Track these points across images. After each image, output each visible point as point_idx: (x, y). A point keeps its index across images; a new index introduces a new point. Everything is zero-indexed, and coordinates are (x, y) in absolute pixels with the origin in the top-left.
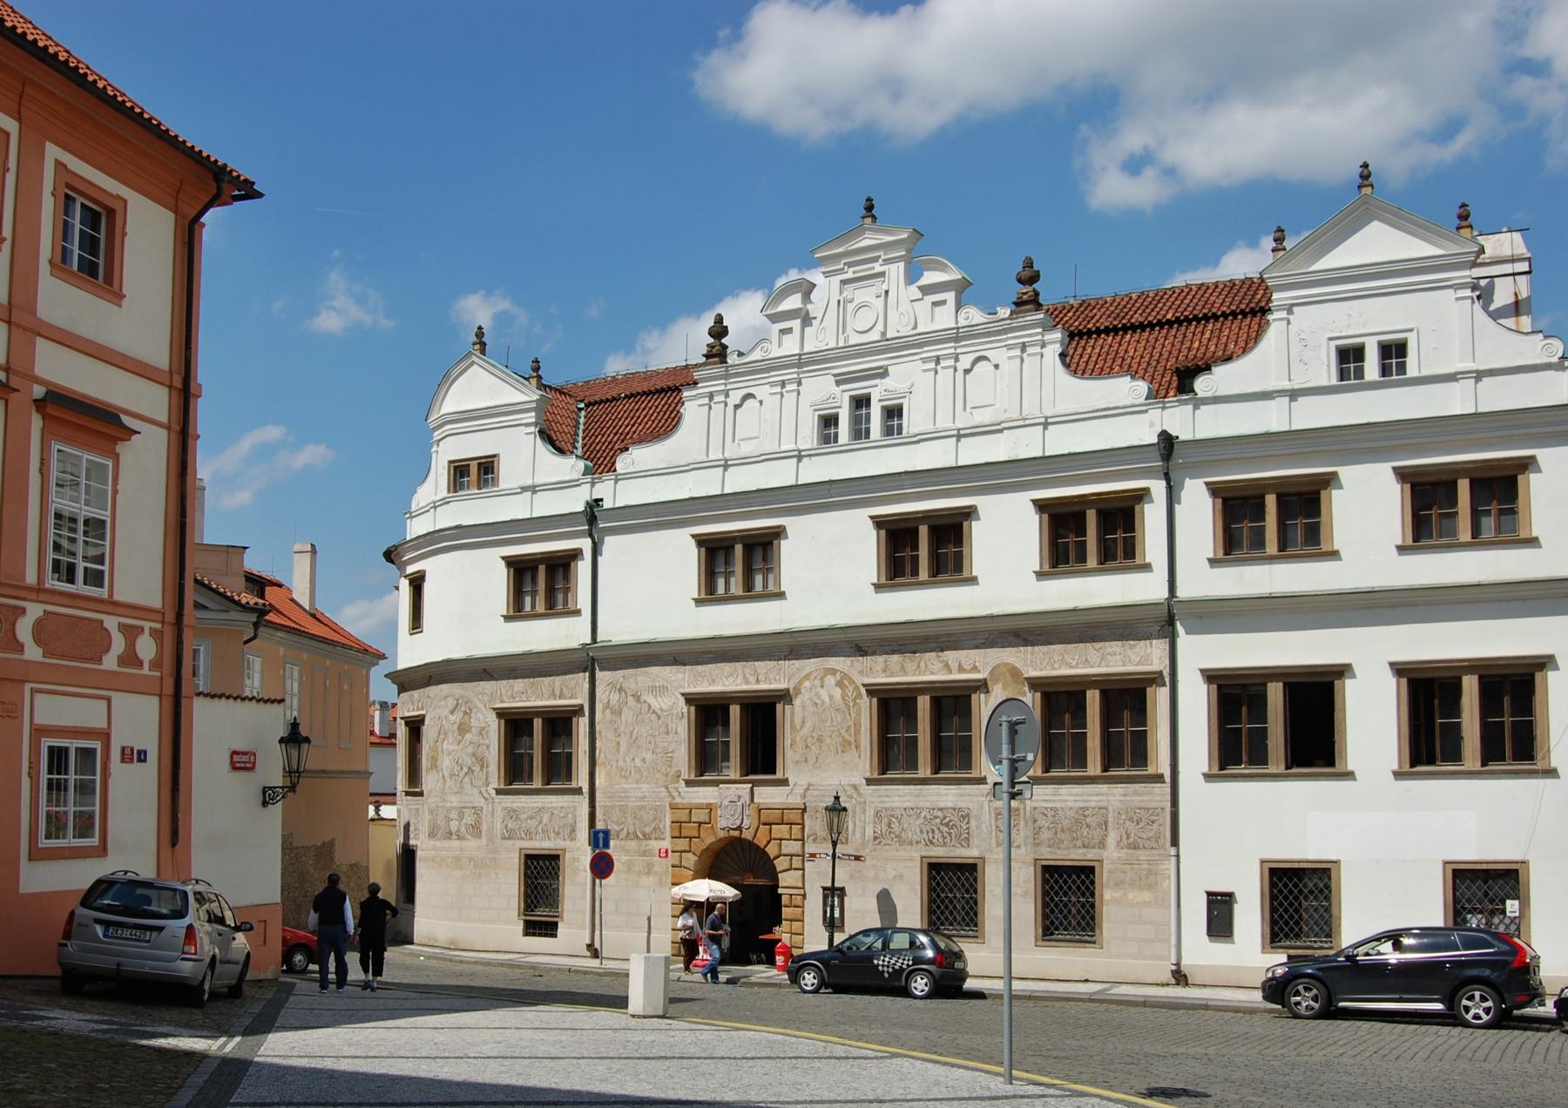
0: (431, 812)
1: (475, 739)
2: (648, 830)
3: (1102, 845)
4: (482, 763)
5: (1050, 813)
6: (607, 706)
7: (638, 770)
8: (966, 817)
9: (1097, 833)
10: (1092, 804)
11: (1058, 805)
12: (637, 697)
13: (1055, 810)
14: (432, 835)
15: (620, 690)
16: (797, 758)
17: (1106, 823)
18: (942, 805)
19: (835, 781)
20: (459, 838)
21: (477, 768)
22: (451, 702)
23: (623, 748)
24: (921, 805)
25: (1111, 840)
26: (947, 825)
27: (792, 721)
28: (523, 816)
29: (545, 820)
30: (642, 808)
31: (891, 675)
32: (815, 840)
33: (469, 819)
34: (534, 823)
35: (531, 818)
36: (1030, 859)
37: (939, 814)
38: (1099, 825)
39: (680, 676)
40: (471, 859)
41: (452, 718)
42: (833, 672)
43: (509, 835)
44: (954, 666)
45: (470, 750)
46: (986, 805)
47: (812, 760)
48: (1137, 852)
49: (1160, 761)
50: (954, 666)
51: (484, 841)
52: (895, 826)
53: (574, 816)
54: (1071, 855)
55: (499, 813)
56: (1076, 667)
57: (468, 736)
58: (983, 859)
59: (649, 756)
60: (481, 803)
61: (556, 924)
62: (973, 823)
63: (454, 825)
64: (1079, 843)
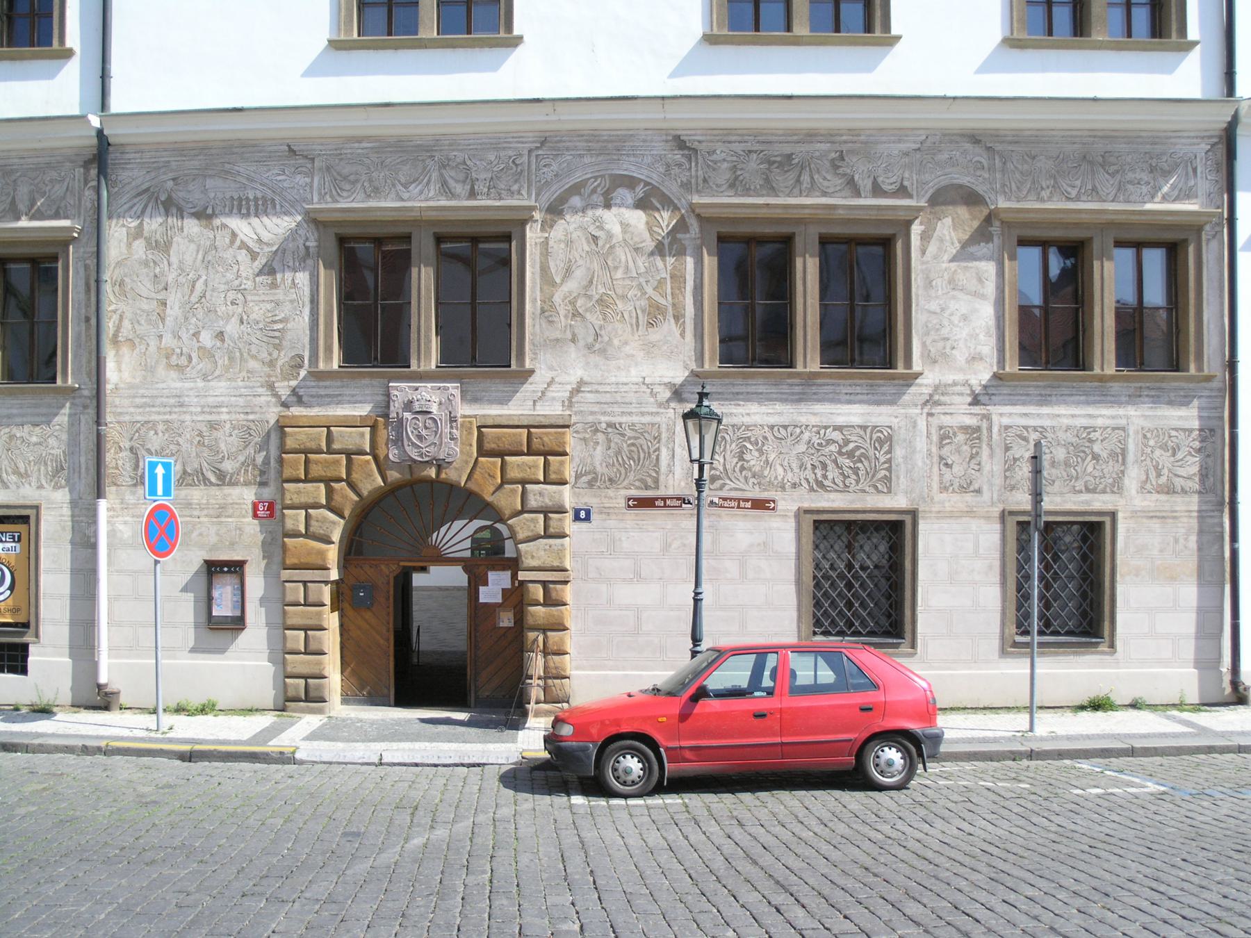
2: (228, 466)
3: (1117, 486)
5: (1034, 436)
8: (886, 440)
9: (1110, 468)
10: (1100, 422)
11: (1047, 423)
13: (1042, 430)
16: (558, 335)
17: (1124, 452)
18: (840, 421)
19: (634, 375)
23: (174, 311)
24: (803, 420)
25: (1132, 479)
26: (850, 455)
27: (544, 269)
30: (213, 426)
31: (747, 192)
32: (591, 484)
36: (996, 510)
37: (836, 436)
38: (1113, 455)
39: (301, 180)
42: (630, 183)
44: (865, 184)
46: (922, 424)
47: (585, 336)
48: (1178, 499)
49: (1213, 361)
50: (865, 184)
52: (753, 459)
54: (1062, 501)
56: (1077, 199)
58: (914, 514)
59: (232, 328)
61: (25, 647)
62: (899, 452)
64: (1079, 485)
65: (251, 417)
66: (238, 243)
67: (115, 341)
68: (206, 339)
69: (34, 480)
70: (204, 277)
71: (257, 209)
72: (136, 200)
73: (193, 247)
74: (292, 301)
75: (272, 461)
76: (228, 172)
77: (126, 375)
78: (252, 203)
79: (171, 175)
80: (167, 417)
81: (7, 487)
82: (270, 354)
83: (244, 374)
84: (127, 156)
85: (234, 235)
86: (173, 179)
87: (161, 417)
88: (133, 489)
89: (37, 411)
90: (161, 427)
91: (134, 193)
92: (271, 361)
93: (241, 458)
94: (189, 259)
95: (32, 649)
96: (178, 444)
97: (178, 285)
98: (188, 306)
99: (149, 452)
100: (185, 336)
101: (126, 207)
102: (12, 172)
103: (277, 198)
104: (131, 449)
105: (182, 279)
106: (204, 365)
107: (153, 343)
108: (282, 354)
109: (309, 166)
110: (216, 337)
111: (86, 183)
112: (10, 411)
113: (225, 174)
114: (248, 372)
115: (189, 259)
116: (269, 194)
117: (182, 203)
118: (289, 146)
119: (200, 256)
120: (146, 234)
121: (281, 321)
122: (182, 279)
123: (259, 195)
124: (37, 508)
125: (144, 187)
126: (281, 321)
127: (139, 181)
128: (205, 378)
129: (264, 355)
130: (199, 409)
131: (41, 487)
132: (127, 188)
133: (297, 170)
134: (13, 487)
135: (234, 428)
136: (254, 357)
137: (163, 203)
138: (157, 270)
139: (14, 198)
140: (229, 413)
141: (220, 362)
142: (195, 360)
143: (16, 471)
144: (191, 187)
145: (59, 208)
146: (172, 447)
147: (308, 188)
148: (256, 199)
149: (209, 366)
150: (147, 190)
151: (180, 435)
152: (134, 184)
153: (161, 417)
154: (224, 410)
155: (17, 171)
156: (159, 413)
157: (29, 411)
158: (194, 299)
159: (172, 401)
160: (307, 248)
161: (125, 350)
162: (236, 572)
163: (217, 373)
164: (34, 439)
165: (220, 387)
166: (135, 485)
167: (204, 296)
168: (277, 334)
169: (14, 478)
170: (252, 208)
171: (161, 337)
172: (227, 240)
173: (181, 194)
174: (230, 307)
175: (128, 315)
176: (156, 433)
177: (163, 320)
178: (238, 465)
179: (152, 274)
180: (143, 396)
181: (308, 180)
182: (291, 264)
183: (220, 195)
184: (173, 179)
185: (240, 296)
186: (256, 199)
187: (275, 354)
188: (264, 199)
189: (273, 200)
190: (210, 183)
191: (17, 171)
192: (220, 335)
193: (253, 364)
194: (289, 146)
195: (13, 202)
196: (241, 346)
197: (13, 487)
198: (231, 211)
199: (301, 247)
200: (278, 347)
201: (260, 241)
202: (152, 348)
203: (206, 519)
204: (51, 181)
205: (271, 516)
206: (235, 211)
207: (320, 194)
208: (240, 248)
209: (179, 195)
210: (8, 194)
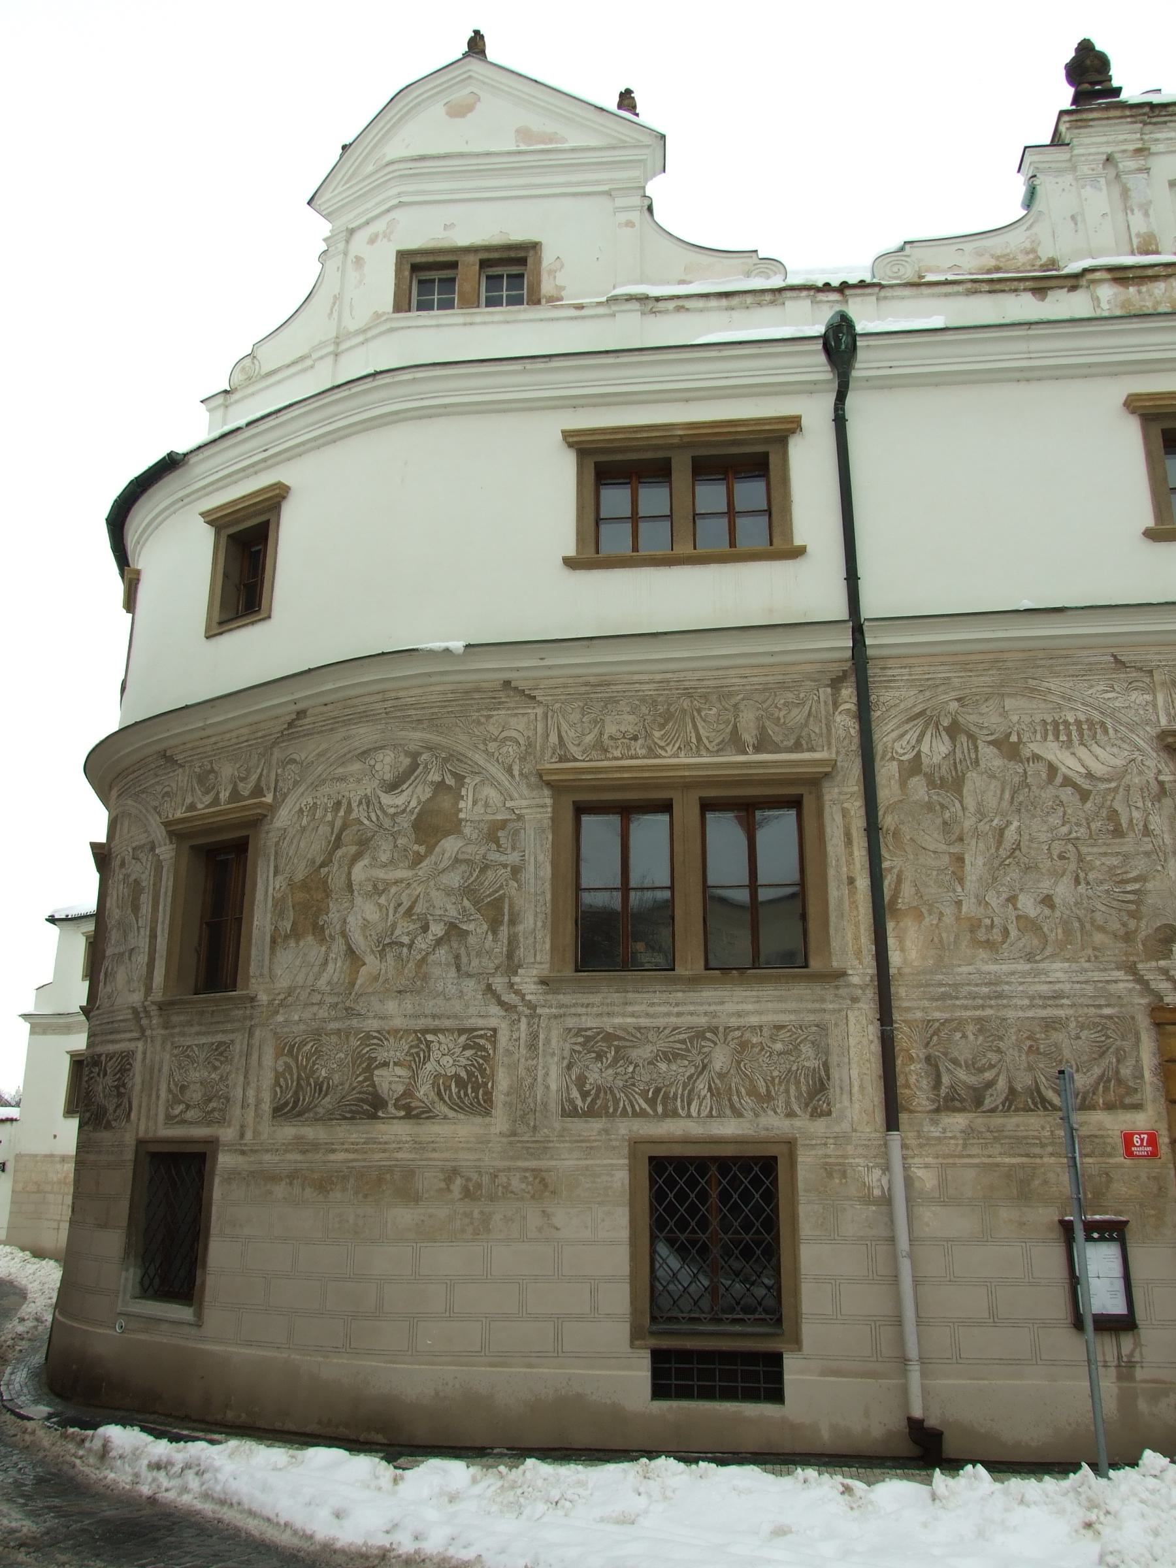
0: (288, 1049)
1: (475, 852)
4: (497, 912)
6: (915, 766)
7: (1029, 925)
12: (1009, 748)
14: (287, 1109)
15: (954, 730)
20: (412, 1113)
21: (477, 927)
22: (387, 763)
28: (643, 1053)
29: (720, 1059)
30: (1050, 1025)
33: (448, 1058)
34: (679, 1070)
35: (670, 1056)
40: (452, 1174)
41: (387, 800)
43: (594, 1104)
45: (454, 879)
51: (500, 1121)
53: (823, 1051)
55: (555, 1041)
57: (450, 846)
59: (1063, 891)
60: (494, 1017)
63: (390, 1081)
65: (1107, 1011)
66: (1059, 780)
67: (895, 912)
68: (1028, 905)
69: (780, 1103)
70: (1016, 824)
71: (1081, 735)
72: (907, 727)
73: (994, 783)
74: (1147, 854)
75: (1147, 1075)
76: (1033, 690)
77: (913, 955)
78: (1073, 728)
79: (954, 695)
80: (978, 1013)
81: (740, 1115)
82: (1124, 925)
83: (1090, 952)
84: (890, 672)
85: (1052, 769)
86: (959, 700)
87: (969, 1013)
88: (935, 1116)
89: (783, 1006)
90: (971, 1029)
91: (904, 717)
92: (1127, 933)
93: (1097, 1071)
94: (991, 801)
95: (790, 1363)
96: (999, 1051)
97: (978, 835)
98: (996, 863)
99: (955, 1062)
100: (994, 901)
101: (894, 735)
102: (730, 695)
103: (1109, 722)
104: (928, 1059)
105: (983, 827)
106: (1030, 941)
107: (949, 911)
108: (1143, 924)
109: (1148, 680)
110: (1043, 901)
111: (836, 705)
112: (740, 1007)
113: (1031, 692)
114: (1094, 949)
115: (991, 801)
116: (1096, 716)
117: (973, 728)
118: (1114, 656)
119: (1007, 796)
120: (925, 769)
121: (1135, 880)
122: (983, 827)
123: (1082, 718)
124: (790, 1144)
125: (917, 710)
126: (1135, 880)
127: (909, 703)
128: (1030, 958)
129: (1115, 926)
130: (1026, 1002)
131: (791, 1114)
132: (893, 712)
133: (1130, 686)
134: (749, 1115)
135: (1082, 1027)
136: (1101, 929)
137: (946, 729)
138: (947, 815)
139: (735, 726)
140: (1072, 1006)
141: (1052, 937)
142: (1014, 933)
143: (753, 1092)
144: (984, 709)
145: (799, 738)
146: (990, 1055)
147: (1150, 708)
148: (1078, 723)
149: (1036, 942)
150: (922, 713)
151: (1001, 1038)
152: (902, 706)
153: (969, 1013)
154: (1065, 1001)
155: (737, 693)
156: (966, 1008)
157: (770, 1005)
158: (1003, 853)
159: (985, 990)
160: (1161, 784)
161: (909, 923)
162: (1111, 1239)
163: (1047, 953)
164: (779, 1046)
165: (1058, 970)
166: (937, 1110)
167: (1018, 847)
168: (1131, 897)
169: (748, 1102)
170: (1074, 734)
171: (959, 903)
172: (1044, 776)
173: (971, 718)
174: (1059, 863)
175: (909, 875)
176: (964, 1036)
177: (961, 880)
178: (1092, 1080)
179: (939, 821)
180: (941, 985)
181: (1148, 697)
182: (1140, 804)
183: (1027, 719)
184: (959, 700)
185: (1070, 847)
186: (1078, 723)
187: (1132, 924)
188: (1091, 723)
189: (1103, 724)
190: (1009, 703)
191: (737, 693)
192: (1047, 901)
193: (1098, 938)
194: (1114, 656)
195: (735, 732)
196: (1081, 913)
197: (749, 1115)
198: (1045, 739)
199: (1153, 783)
200: (1135, 915)
201: (1090, 775)
202: (949, 920)
203: (1052, 1160)
204: (784, 704)
205: (1154, 1154)
206: (1050, 737)
207: (1168, 714)
208: (1063, 785)
209: (969, 719)
210: (727, 722)
